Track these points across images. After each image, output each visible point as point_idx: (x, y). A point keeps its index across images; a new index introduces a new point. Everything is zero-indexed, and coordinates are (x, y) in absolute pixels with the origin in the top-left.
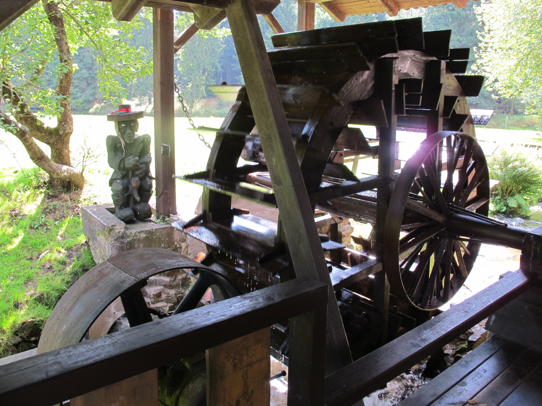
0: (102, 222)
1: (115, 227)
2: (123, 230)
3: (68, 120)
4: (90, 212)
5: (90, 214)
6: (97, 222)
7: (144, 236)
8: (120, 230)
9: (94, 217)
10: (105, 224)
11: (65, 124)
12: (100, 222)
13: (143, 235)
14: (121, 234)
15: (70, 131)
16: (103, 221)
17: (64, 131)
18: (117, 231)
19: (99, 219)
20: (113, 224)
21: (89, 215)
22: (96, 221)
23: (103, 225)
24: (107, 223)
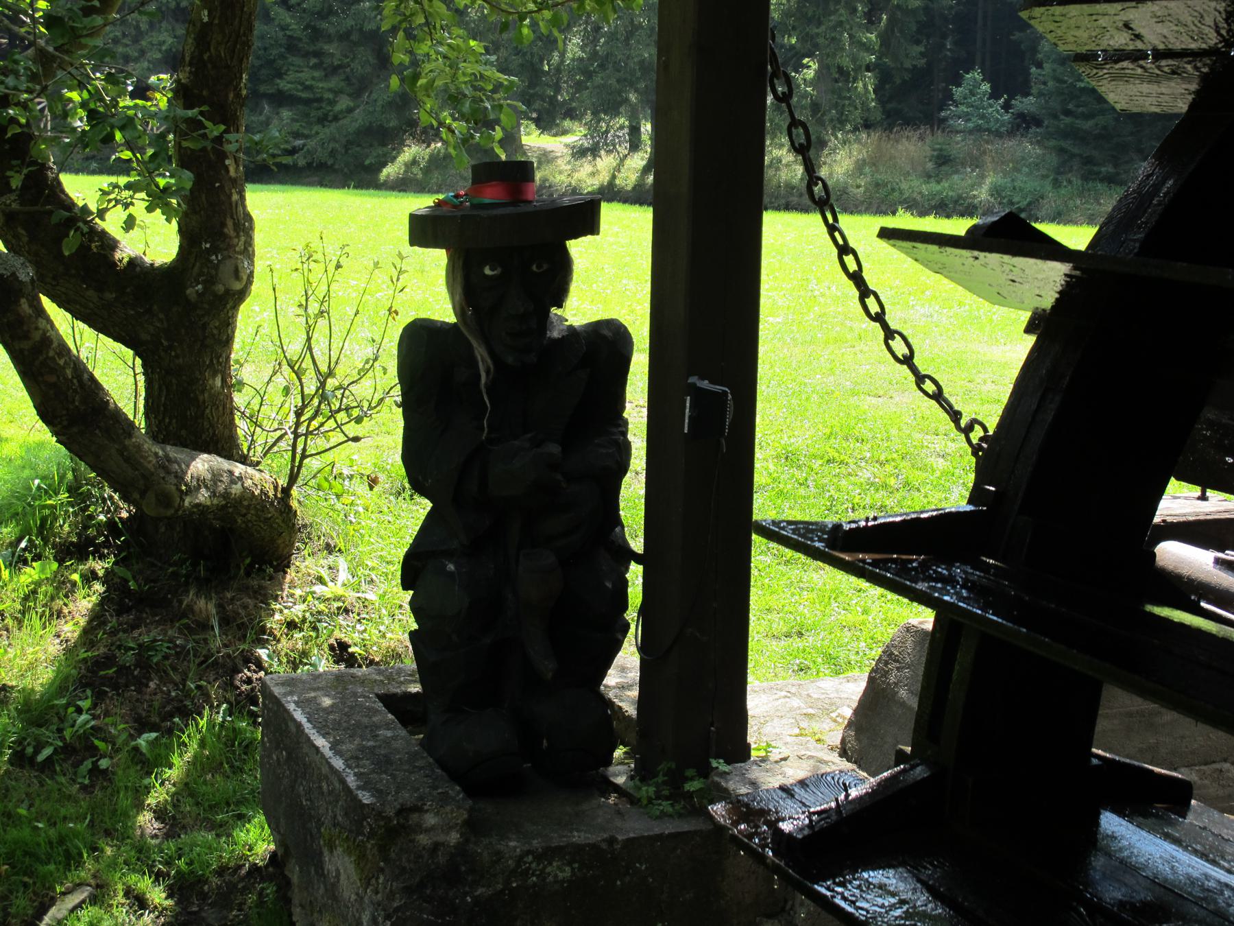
0: (351, 781)
1: (415, 817)
2: (454, 837)
3: (229, 230)
4: (299, 716)
5: (299, 725)
6: (326, 778)
7: (567, 873)
8: (441, 838)
9: (317, 749)
10: (366, 798)
11: (215, 250)
12: (343, 782)
13: (560, 872)
14: (442, 859)
15: (238, 286)
16: (358, 776)
17: (210, 281)
18: (423, 840)
19: (338, 763)
20: (407, 797)
21: (293, 729)
22: (325, 770)
23: (355, 799)
24: (378, 793)
